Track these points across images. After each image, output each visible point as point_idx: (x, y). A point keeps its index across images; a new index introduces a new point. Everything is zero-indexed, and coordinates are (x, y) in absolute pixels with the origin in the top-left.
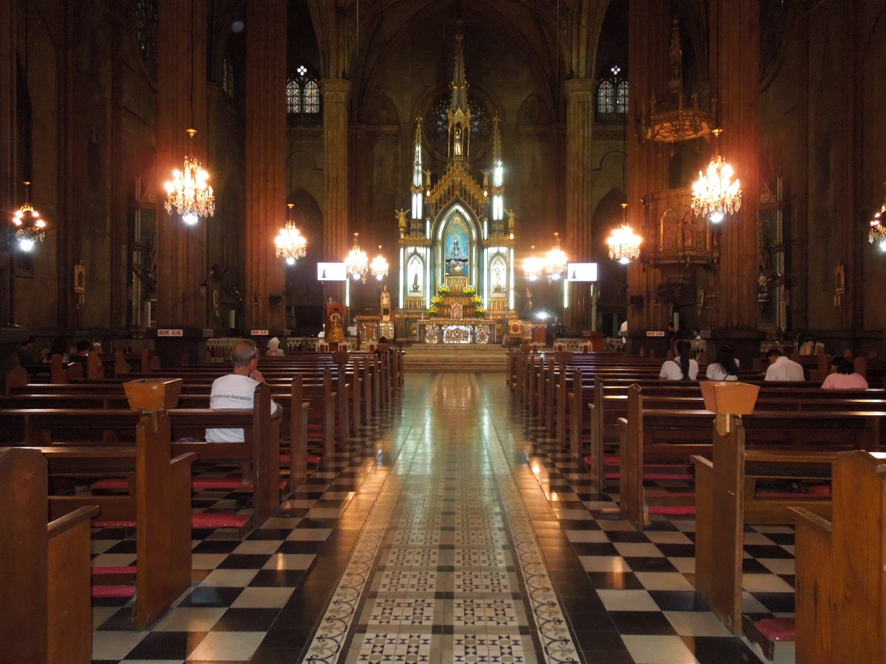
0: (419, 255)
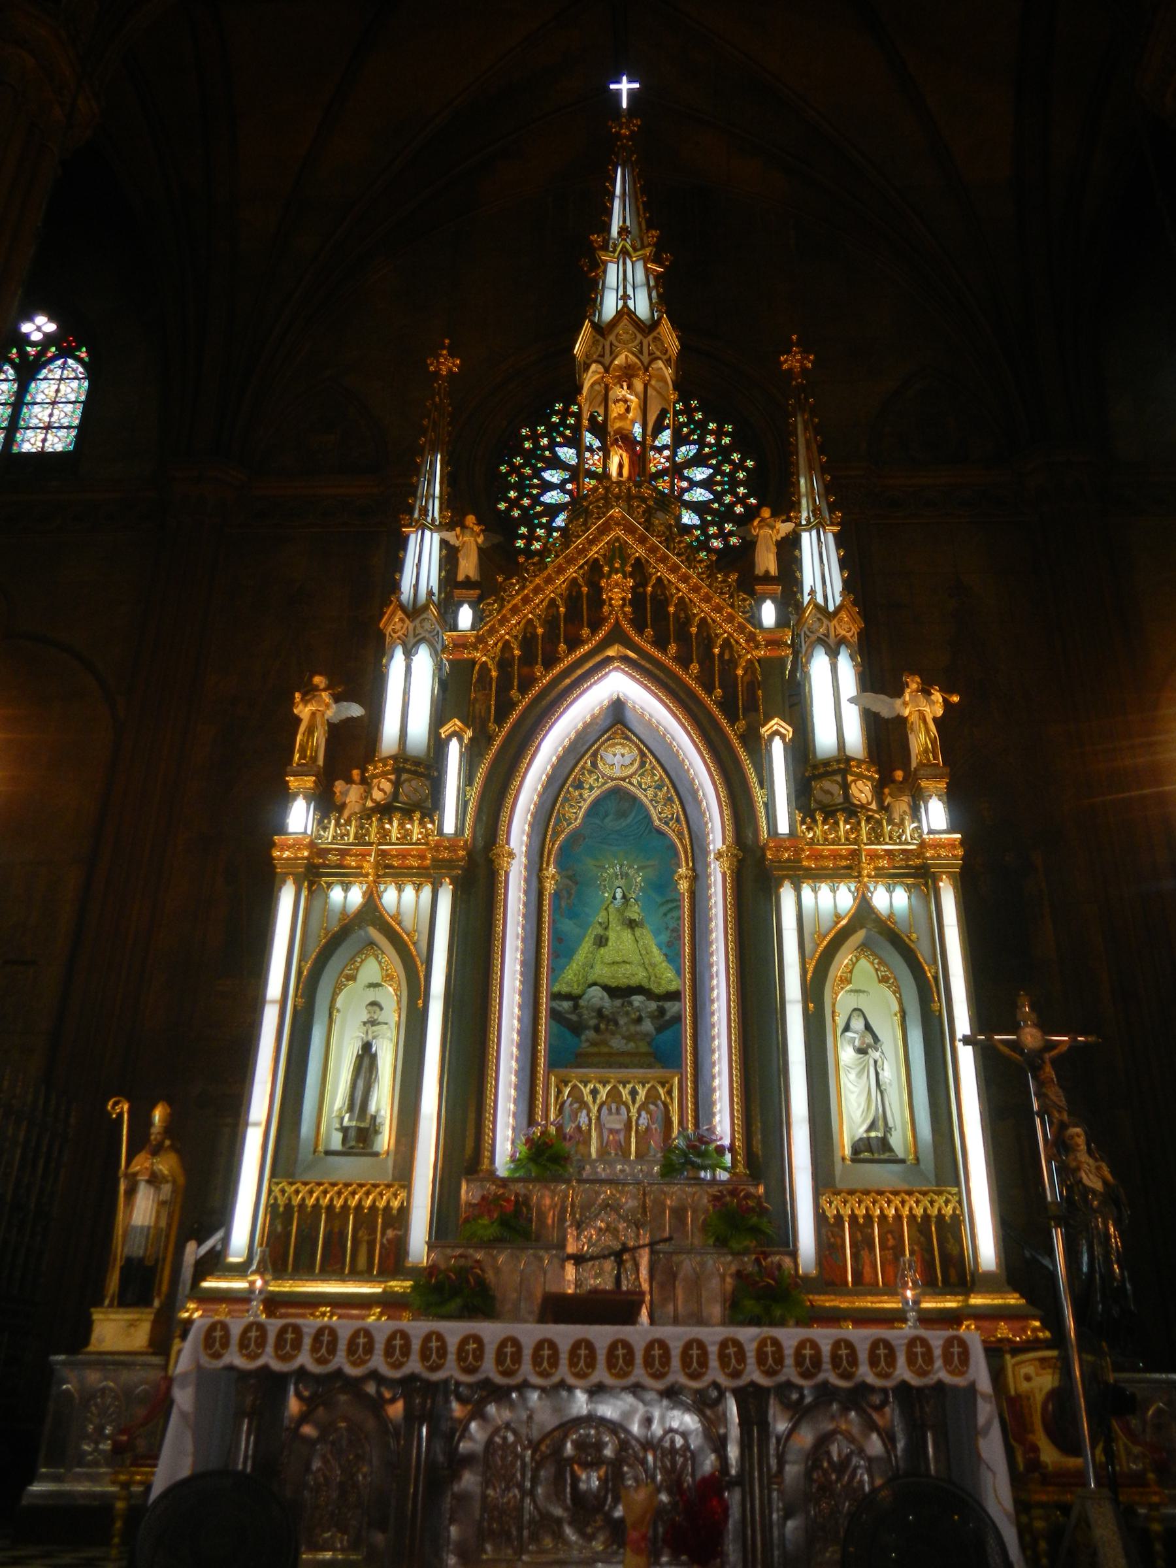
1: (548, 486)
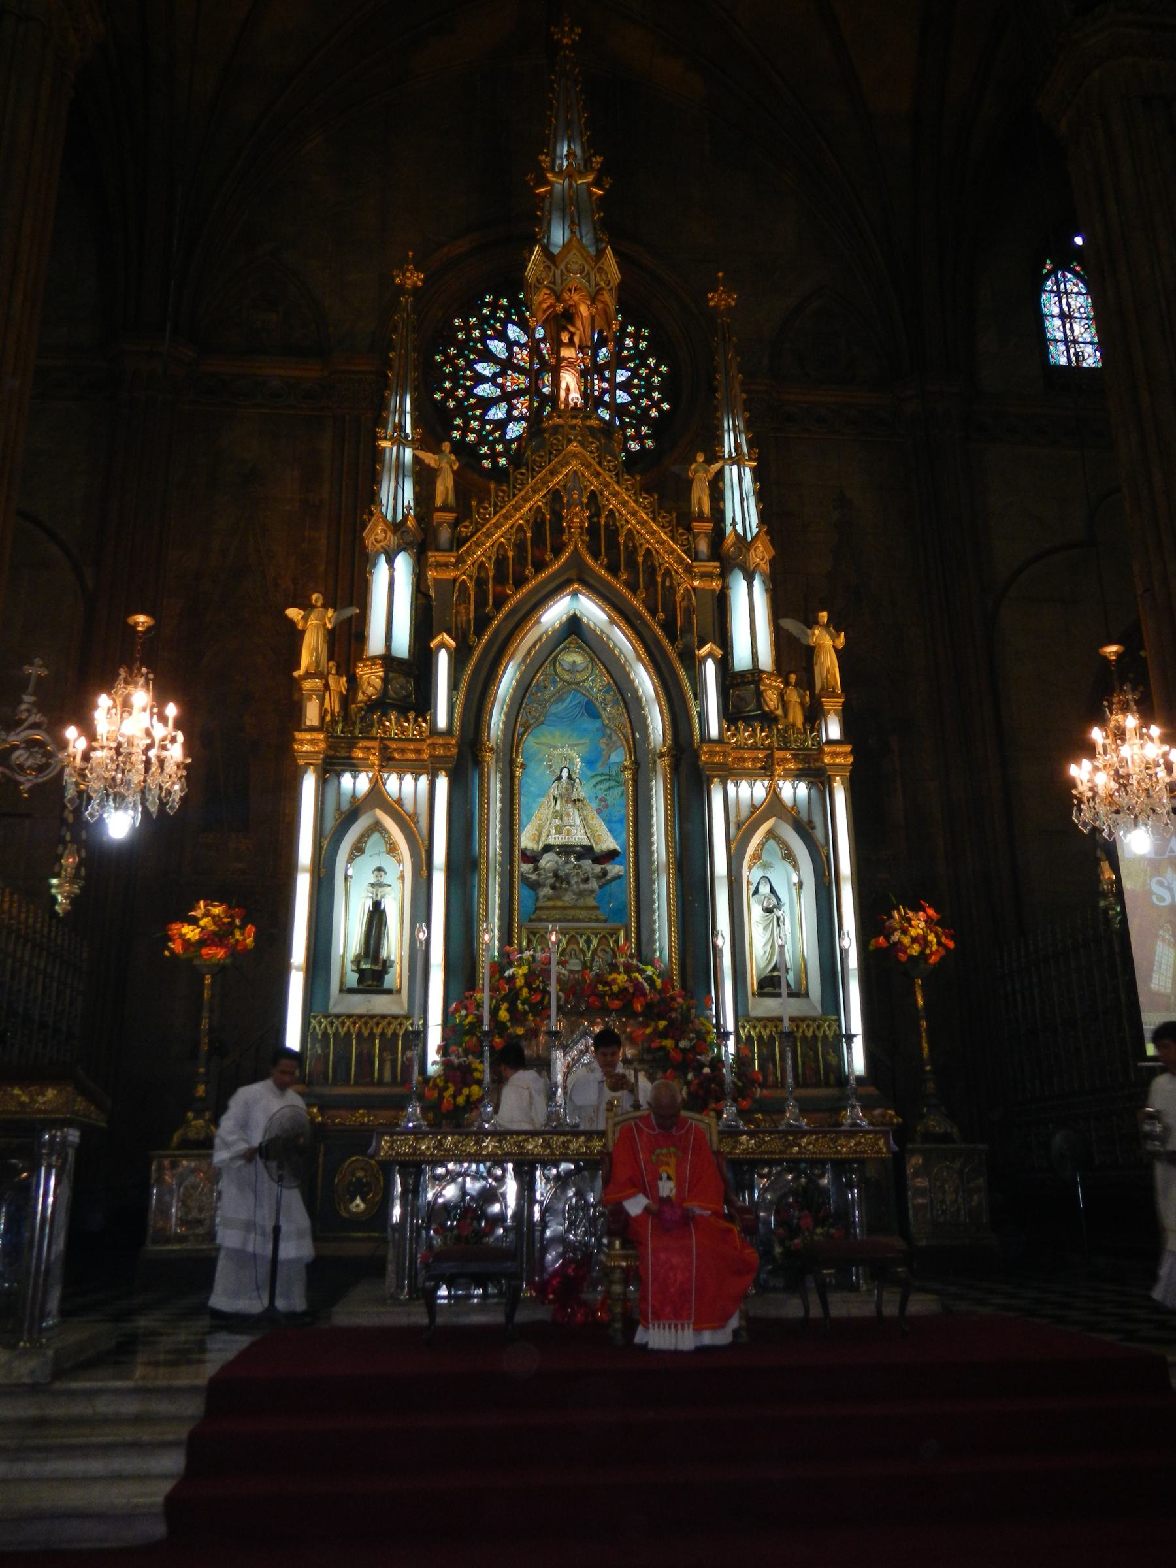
0: (394, 809)
1: (480, 379)
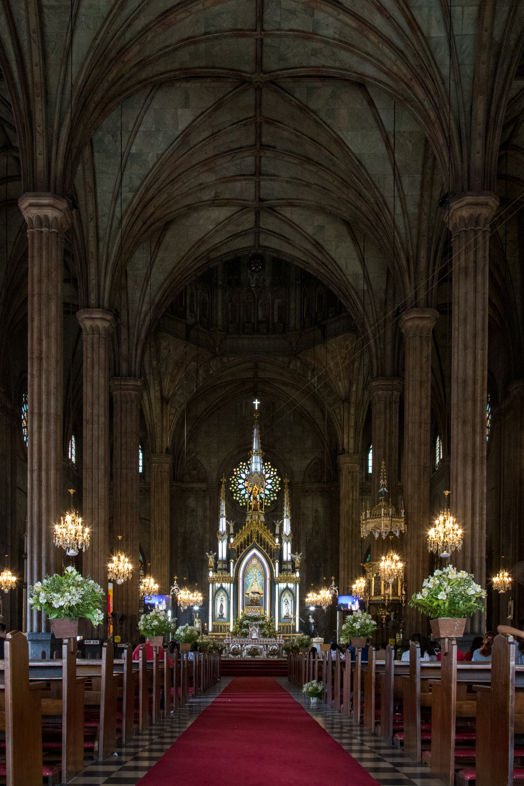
1: (239, 484)
